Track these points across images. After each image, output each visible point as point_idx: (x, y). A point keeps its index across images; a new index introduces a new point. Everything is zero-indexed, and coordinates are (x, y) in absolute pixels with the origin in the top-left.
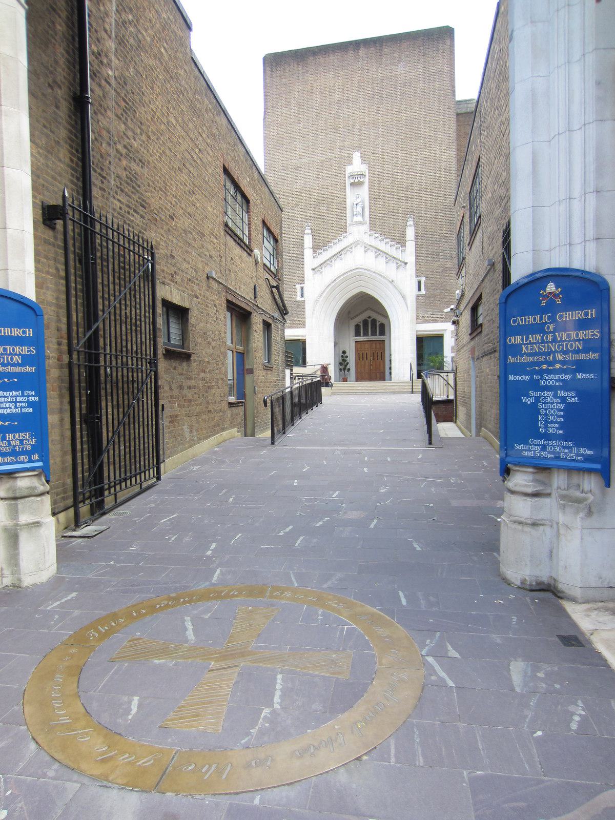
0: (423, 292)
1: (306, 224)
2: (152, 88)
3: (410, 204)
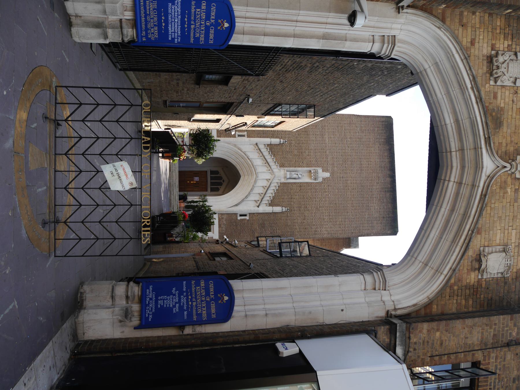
2: (352, 78)
3: (295, 209)
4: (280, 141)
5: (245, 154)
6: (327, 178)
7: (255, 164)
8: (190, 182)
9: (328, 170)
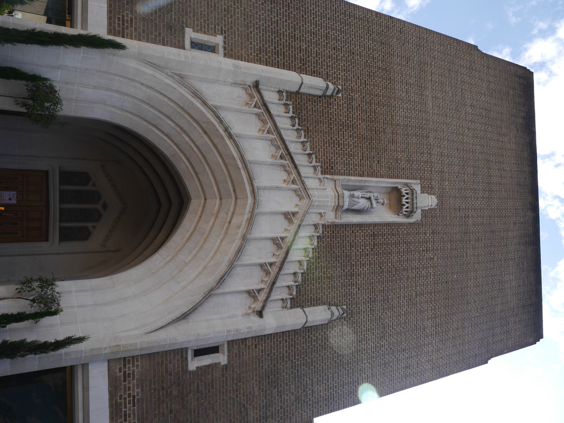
1: (340, 87)
4: (327, 87)
5: (218, 117)
6: (430, 210)
7: (249, 157)
9: (432, 188)
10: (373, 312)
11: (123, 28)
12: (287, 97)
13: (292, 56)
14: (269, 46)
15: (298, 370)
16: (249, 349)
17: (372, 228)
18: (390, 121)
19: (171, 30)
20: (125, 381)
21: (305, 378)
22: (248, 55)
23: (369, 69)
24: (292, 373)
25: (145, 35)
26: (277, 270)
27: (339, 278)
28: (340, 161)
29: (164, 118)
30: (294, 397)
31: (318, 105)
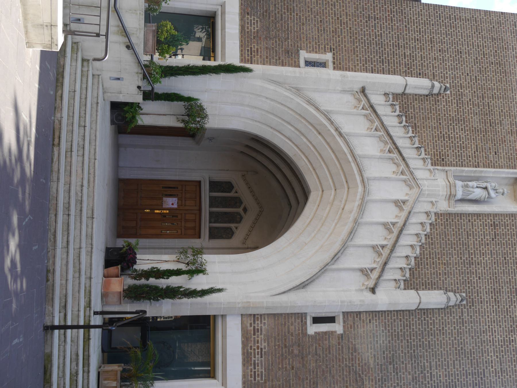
0: (313, 329)
1: (448, 85)
3: (485, 297)
4: (433, 86)
5: (329, 120)
7: (358, 151)
8: (153, 210)
10: (498, 303)
11: (251, 57)
12: (393, 98)
13: (397, 62)
14: (374, 57)
15: (414, 351)
16: (363, 322)
17: (492, 218)
18: (507, 112)
19: (288, 53)
20: (254, 334)
21: (422, 359)
22: (355, 66)
23: (480, 65)
24: (408, 353)
25: (268, 60)
26: (389, 252)
27: (456, 265)
28: (451, 154)
29: (286, 124)
30: (411, 376)
31: (425, 103)
